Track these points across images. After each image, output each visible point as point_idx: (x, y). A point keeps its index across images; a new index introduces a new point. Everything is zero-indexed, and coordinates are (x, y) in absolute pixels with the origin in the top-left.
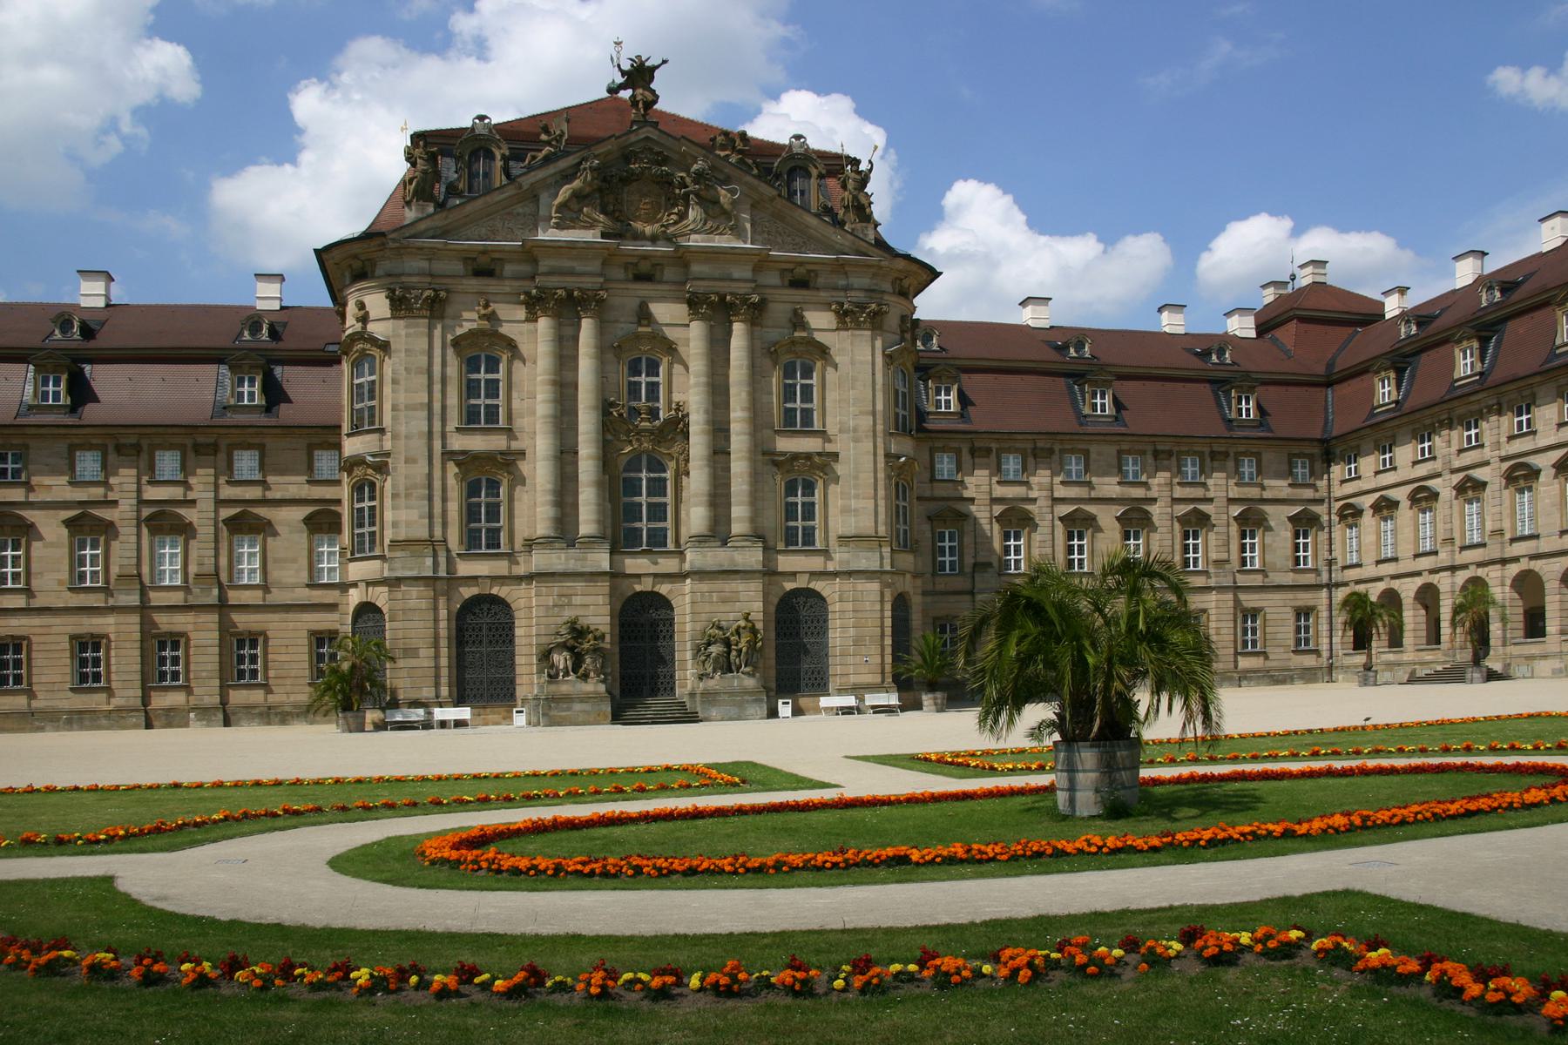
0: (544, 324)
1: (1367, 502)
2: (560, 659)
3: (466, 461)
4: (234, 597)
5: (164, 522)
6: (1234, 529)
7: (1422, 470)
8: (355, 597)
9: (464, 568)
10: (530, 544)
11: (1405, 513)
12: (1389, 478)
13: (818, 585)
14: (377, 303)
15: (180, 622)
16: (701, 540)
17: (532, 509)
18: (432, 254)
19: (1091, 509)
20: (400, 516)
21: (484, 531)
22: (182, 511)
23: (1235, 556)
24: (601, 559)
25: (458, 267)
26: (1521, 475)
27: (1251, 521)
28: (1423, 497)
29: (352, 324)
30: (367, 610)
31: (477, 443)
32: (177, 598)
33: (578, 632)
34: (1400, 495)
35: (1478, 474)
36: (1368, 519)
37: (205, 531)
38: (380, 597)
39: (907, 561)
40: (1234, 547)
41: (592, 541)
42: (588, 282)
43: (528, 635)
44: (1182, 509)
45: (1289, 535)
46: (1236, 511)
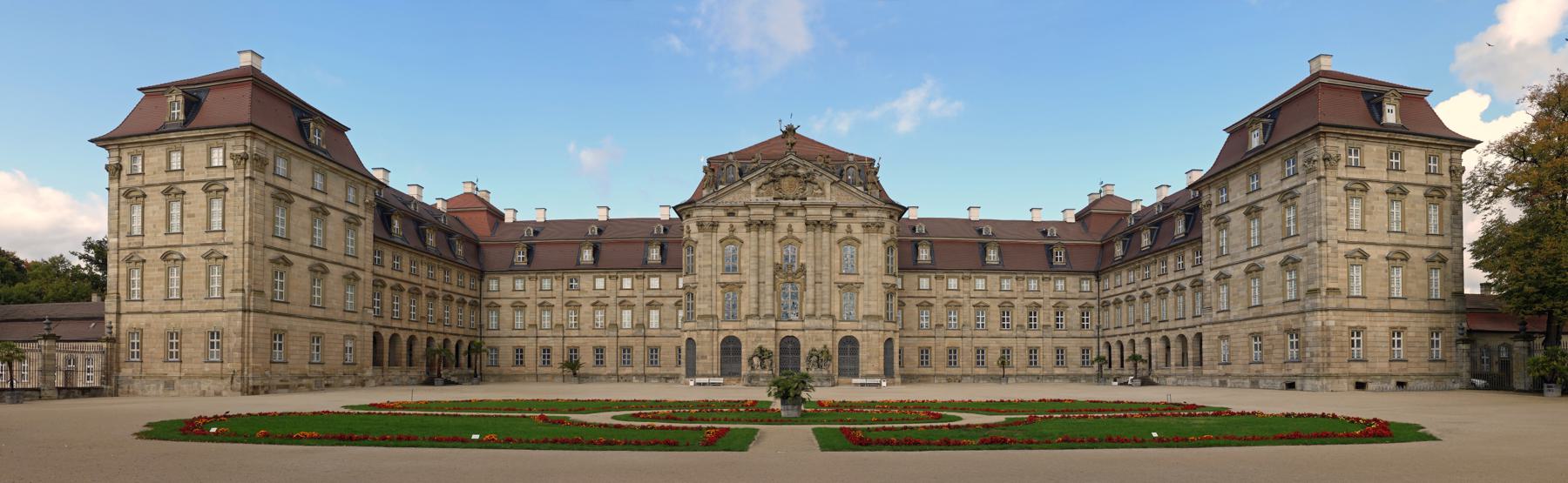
0: (753, 234)
1: (1112, 300)
2: (756, 360)
3: (725, 285)
4: (648, 332)
5: (623, 304)
6: (1052, 312)
7: (1130, 288)
8: (686, 336)
9: (724, 326)
10: (748, 317)
11: (1124, 305)
12: (1119, 290)
13: (854, 334)
14: (694, 227)
15: (631, 342)
16: (810, 316)
17: (746, 307)
18: (713, 208)
19: (987, 302)
20: (702, 307)
21: (731, 313)
22: (633, 301)
23: (1052, 323)
24: (772, 324)
25: (722, 213)
26: (1162, 293)
27: (1059, 310)
28: (1130, 300)
29: (685, 235)
30: (690, 340)
31: (728, 279)
32: (630, 333)
33: (761, 350)
34: (1122, 298)
35: (1149, 291)
36: (1112, 308)
37: (639, 308)
38: (694, 336)
39: (889, 326)
40: (1053, 319)
41: (767, 317)
42: (770, 218)
43: (746, 351)
44: (1029, 302)
45: (1078, 314)
46: (1053, 302)
